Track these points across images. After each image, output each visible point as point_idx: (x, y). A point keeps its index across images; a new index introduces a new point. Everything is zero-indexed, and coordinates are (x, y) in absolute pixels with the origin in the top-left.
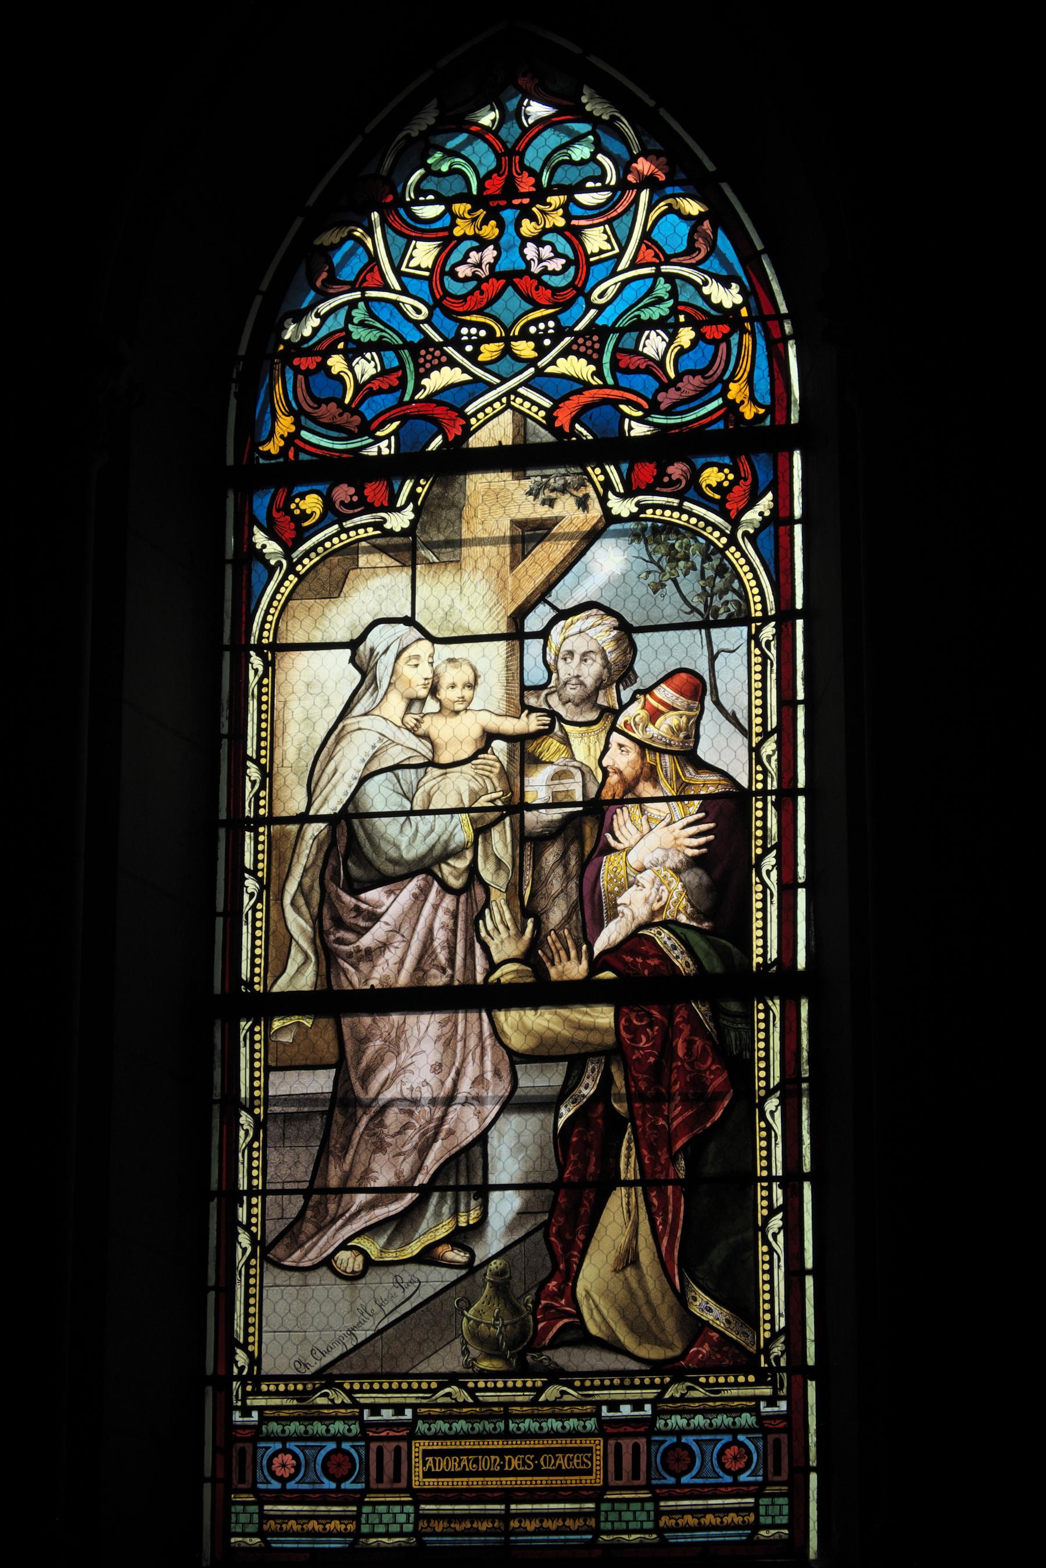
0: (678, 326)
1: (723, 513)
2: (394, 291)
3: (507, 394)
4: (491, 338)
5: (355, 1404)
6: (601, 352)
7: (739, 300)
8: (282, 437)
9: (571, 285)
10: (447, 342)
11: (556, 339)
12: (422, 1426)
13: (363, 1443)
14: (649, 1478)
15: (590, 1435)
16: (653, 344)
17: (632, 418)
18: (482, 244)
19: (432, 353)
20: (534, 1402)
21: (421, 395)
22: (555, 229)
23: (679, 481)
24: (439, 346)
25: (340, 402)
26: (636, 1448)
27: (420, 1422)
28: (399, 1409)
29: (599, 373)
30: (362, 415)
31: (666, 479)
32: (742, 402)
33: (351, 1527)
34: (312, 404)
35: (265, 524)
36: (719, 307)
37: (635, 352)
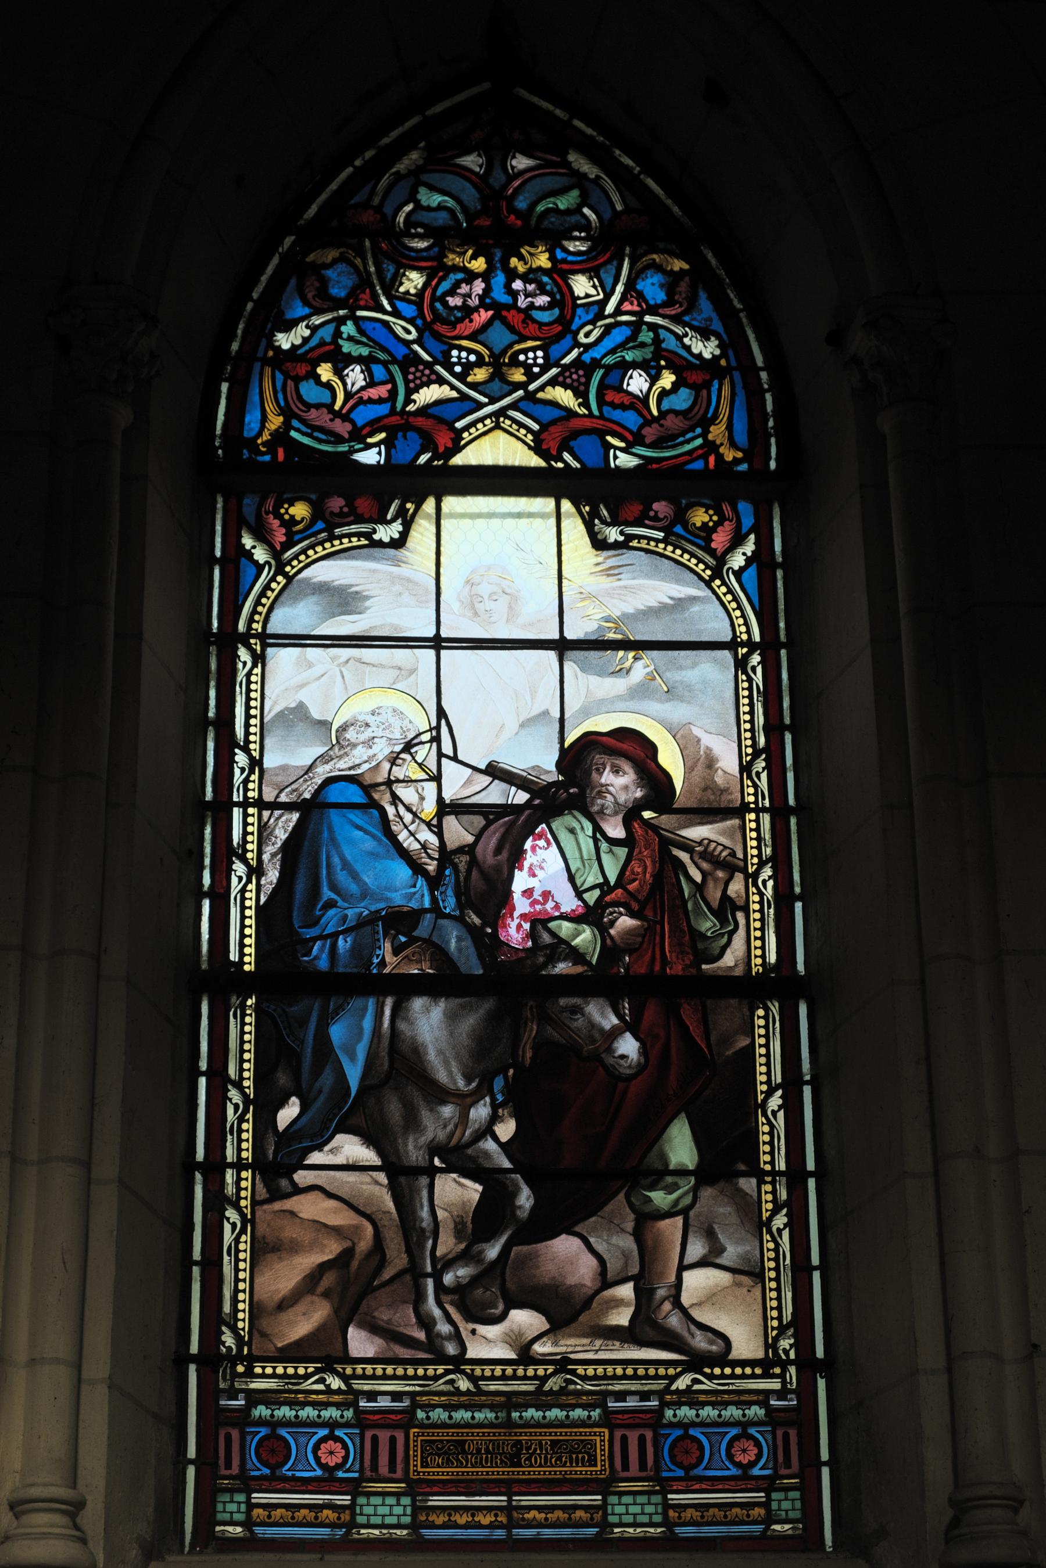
0: (659, 370)
2: (385, 312)
4: (480, 363)
6: (587, 385)
7: (717, 352)
10: (436, 362)
11: (545, 369)
12: (420, 1414)
13: (357, 1431)
15: (595, 1425)
16: (637, 383)
17: (616, 448)
19: (422, 372)
21: (411, 408)
24: (429, 365)
25: (330, 407)
27: (419, 1411)
30: (352, 422)
32: (722, 444)
33: (346, 1517)
34: (304, 409)
36: (699, 356)
37: (619, 389)
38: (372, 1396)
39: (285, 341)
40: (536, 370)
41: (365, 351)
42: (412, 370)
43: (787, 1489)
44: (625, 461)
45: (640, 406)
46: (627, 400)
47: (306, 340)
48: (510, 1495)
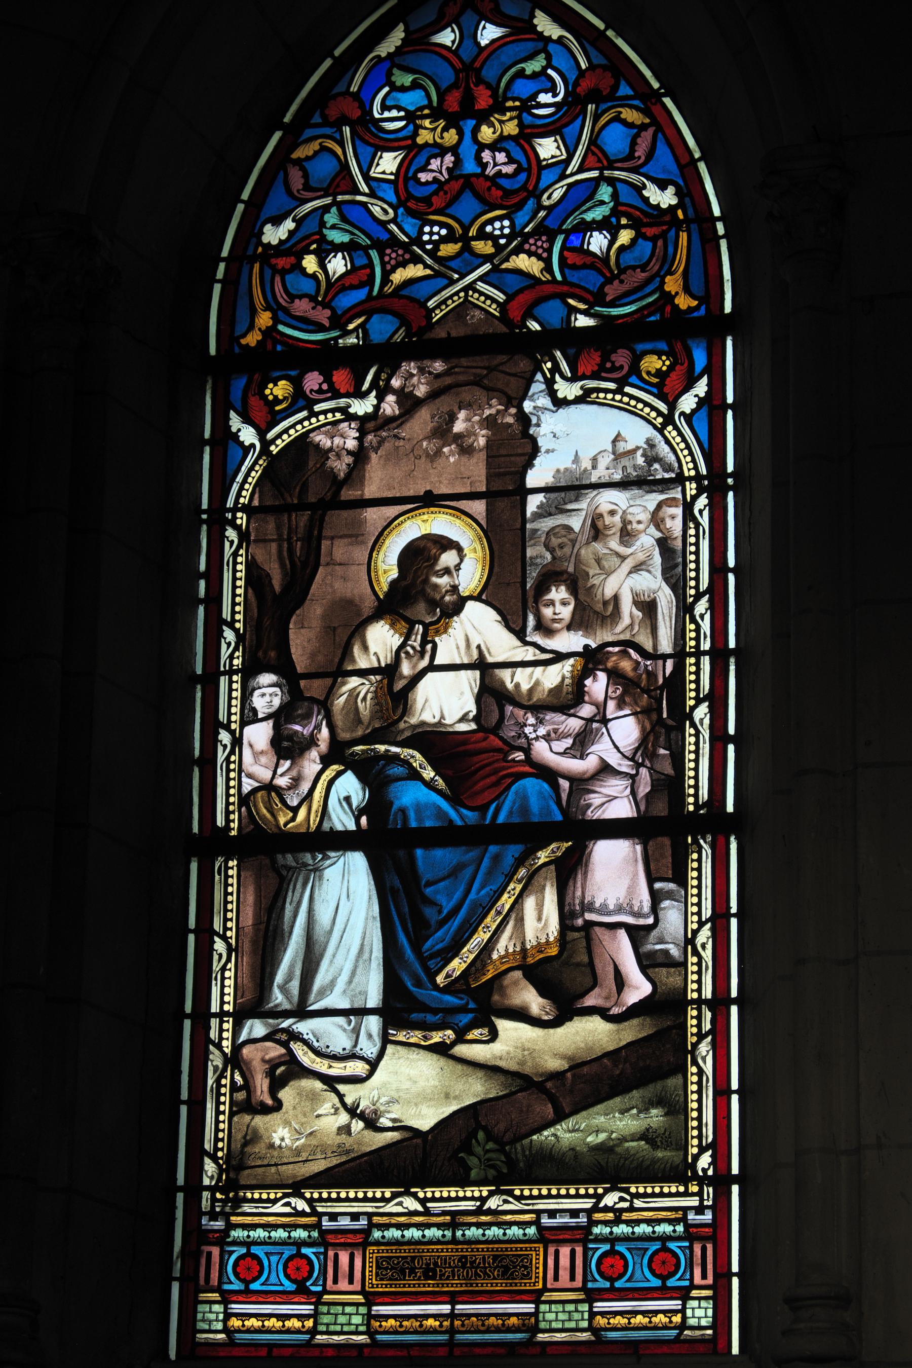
1: (661, 397)
3: (465, 289)
5: (314, 1213)
6: (550, 251)
8: (260, 329)
9: (524, 187)
12: (377, 1234)
14: (585, 1281)
16: (597, 242)
18: (441, 150)
20: (479, 1211)
21: (388, 289)
22: (510, 137)
23: (622, 367)
26: (573, 1253)
28: (355, 1217)
29: (548, 268)
31: (608, 365)
35: (240, 409)
38: (333, 1217)
39: (274, 235)
40: (502, 241)
41: (346, 238)
42: (388, 251)
43: (699, 1299)
44: (583, 321)
45: (599, 265)
46: (589, 260)
47: (291, 233)
48: (453, 1303)
